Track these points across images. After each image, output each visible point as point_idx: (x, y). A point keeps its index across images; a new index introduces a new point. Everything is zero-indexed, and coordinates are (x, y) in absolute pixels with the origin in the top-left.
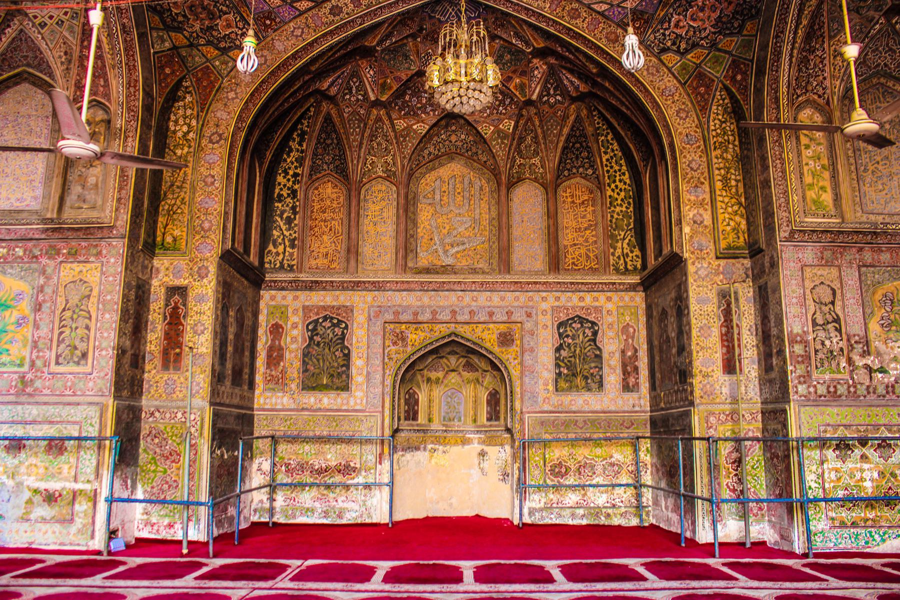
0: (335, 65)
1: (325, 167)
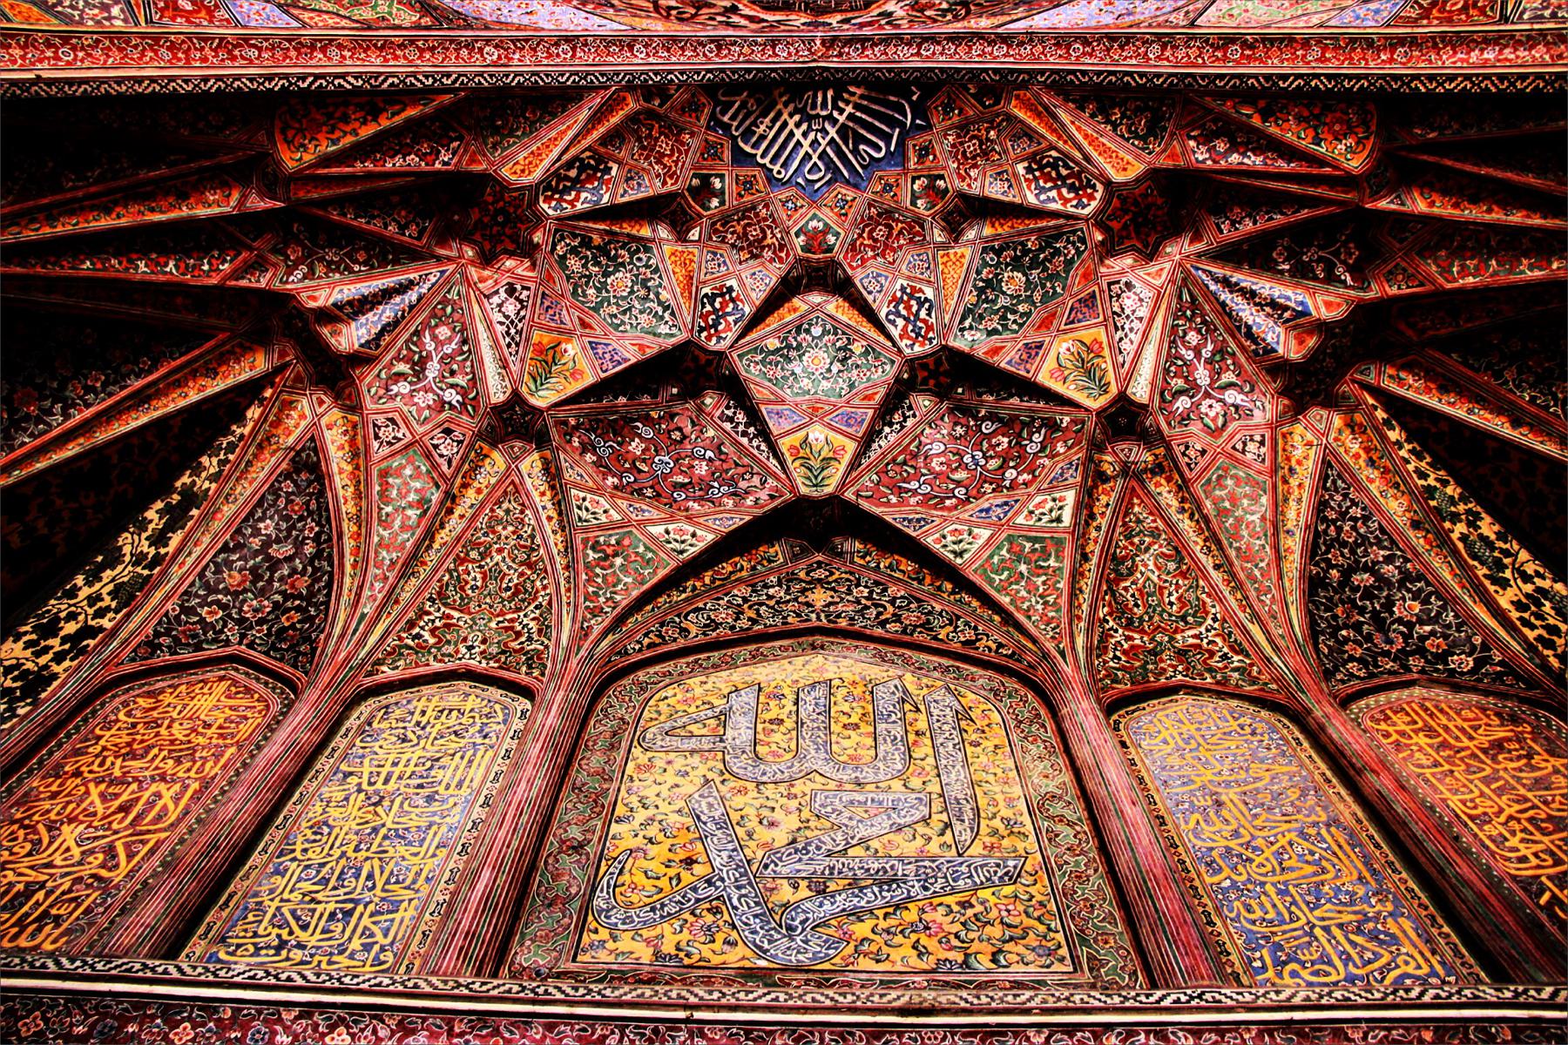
0: (376, 226)
1: (232, 632)
